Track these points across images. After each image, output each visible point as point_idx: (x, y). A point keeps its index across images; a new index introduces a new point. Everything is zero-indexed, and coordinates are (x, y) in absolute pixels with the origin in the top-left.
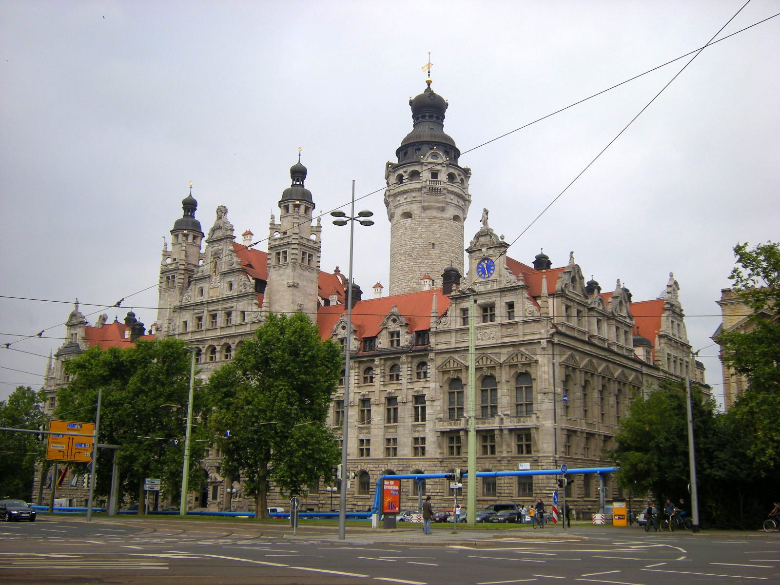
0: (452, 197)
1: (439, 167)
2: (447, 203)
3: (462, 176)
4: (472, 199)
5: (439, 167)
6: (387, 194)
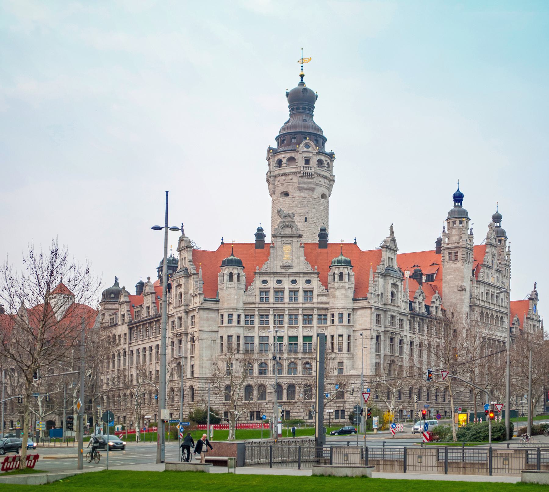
0: (320, 179)
1: (311, 155)
2: (317, 185)
3: (329, 161)
4: (335, 178)
5: (311, 155)
6: (269, 174)
